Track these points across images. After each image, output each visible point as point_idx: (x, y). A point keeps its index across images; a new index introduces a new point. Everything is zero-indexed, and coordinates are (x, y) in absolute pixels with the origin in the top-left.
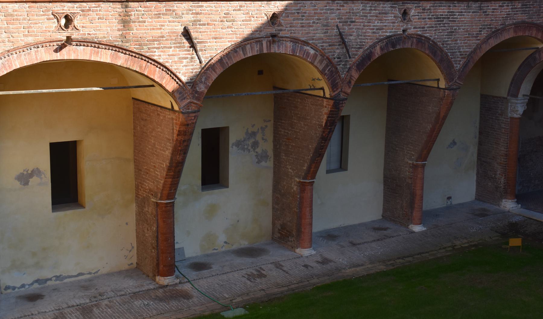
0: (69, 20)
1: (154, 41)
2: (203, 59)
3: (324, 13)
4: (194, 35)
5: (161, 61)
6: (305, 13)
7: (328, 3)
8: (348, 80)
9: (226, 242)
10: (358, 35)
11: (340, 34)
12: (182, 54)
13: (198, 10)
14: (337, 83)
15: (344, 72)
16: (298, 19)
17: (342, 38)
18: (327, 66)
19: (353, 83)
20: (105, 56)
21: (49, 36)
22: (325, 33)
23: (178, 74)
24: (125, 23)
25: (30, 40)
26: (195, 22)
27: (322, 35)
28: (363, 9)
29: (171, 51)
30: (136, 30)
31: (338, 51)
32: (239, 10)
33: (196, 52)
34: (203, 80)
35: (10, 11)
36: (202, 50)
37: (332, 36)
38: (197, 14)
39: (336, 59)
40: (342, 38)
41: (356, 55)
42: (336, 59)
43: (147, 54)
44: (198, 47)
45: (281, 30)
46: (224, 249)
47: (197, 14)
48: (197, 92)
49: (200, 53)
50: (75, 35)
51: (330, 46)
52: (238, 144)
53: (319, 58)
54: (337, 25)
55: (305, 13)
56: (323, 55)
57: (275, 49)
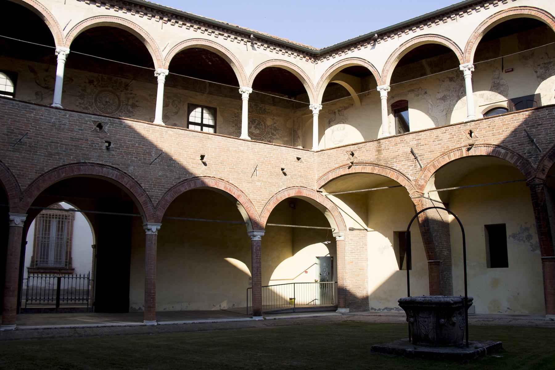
0: (353, 154)
1: (394, 158)
2: (422, 166)
3: (512, 123)
4: (415, 151)
5: (397, 169)
6: (495, 126)
7: (514, 116)
8: (541, 169)
9: (508, 308)
10: (547, 134)
11: (528, 135)
12: (409, 164)
13: (420, 137)
14: (530, 172)
15: (536, 163)
16: (489, 131)
17: (530, 138)
18: (518, 160)
19: (547, 171)
20: (368, 169)
21: (345, 163)
22: (514, 136)
23: (407, 175)
24: (379, 151)
25: (337, 166)
26: (417, 145)
27: (512, 139)
28: (548, 114)
29: (403, 163)
30: (385, 154)
31: (528, 148)
32: (445, 133)
33: (418, 161)
34: (423, 177)
35: (329, 154)
36: (421, 160)
37: (521, 138)
38: (418, 140)
39: (527, 154)
40: (530, 138)
41: (547, 149)
42: (527, 154)
43: (390, 166)
44: (419, 158)
45: (476, 140)
46: (507, 313)
47: (418, 140)
48: (419, 185)
49: (420, 162)
50: (355, 161)
51: (519, 145)
52: (514, 236)
53: (510, 155)
54: (525, 130)
55: (495, 126)
56: (512, 152)
57: (472, 153)
